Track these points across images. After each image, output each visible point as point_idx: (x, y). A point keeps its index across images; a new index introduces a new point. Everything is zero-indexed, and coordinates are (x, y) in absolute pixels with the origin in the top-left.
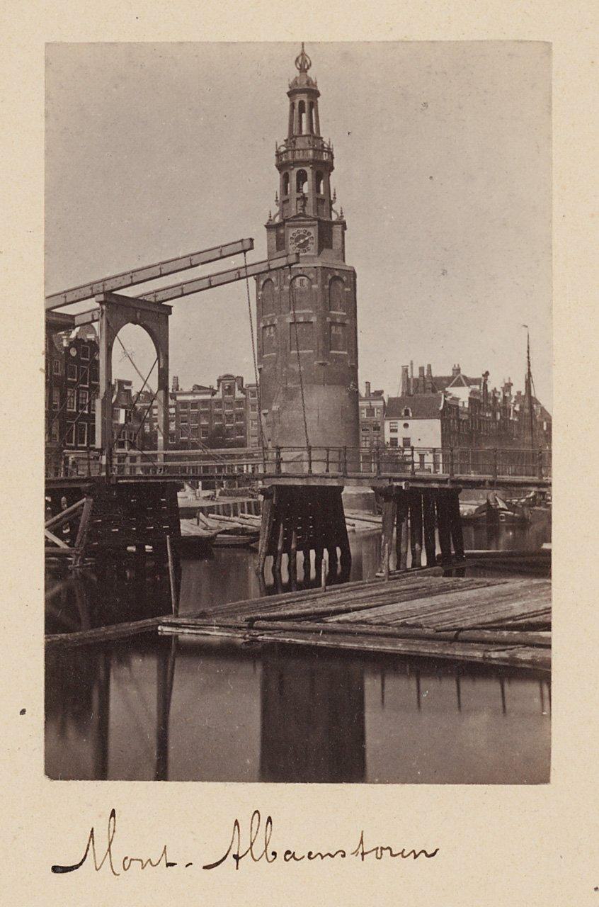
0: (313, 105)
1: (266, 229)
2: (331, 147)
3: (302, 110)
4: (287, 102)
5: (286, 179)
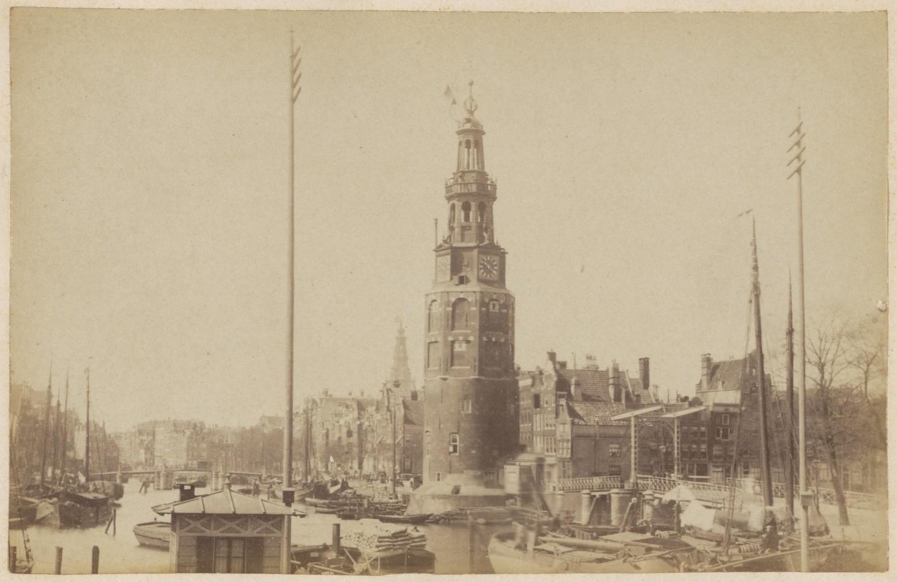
0: (478, 144)
2: (494, 180)
3: (468, 147)
4: (456, 139)
5: (453, 208)
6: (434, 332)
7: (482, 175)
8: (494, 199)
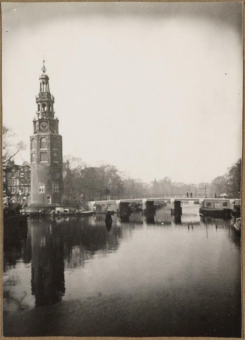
0: (47, 83)
1: (33, 122)
2: (53, 96)
3: (44, 84)
6: (33, 150)
7: (49, 94)
8: (54, 102)
